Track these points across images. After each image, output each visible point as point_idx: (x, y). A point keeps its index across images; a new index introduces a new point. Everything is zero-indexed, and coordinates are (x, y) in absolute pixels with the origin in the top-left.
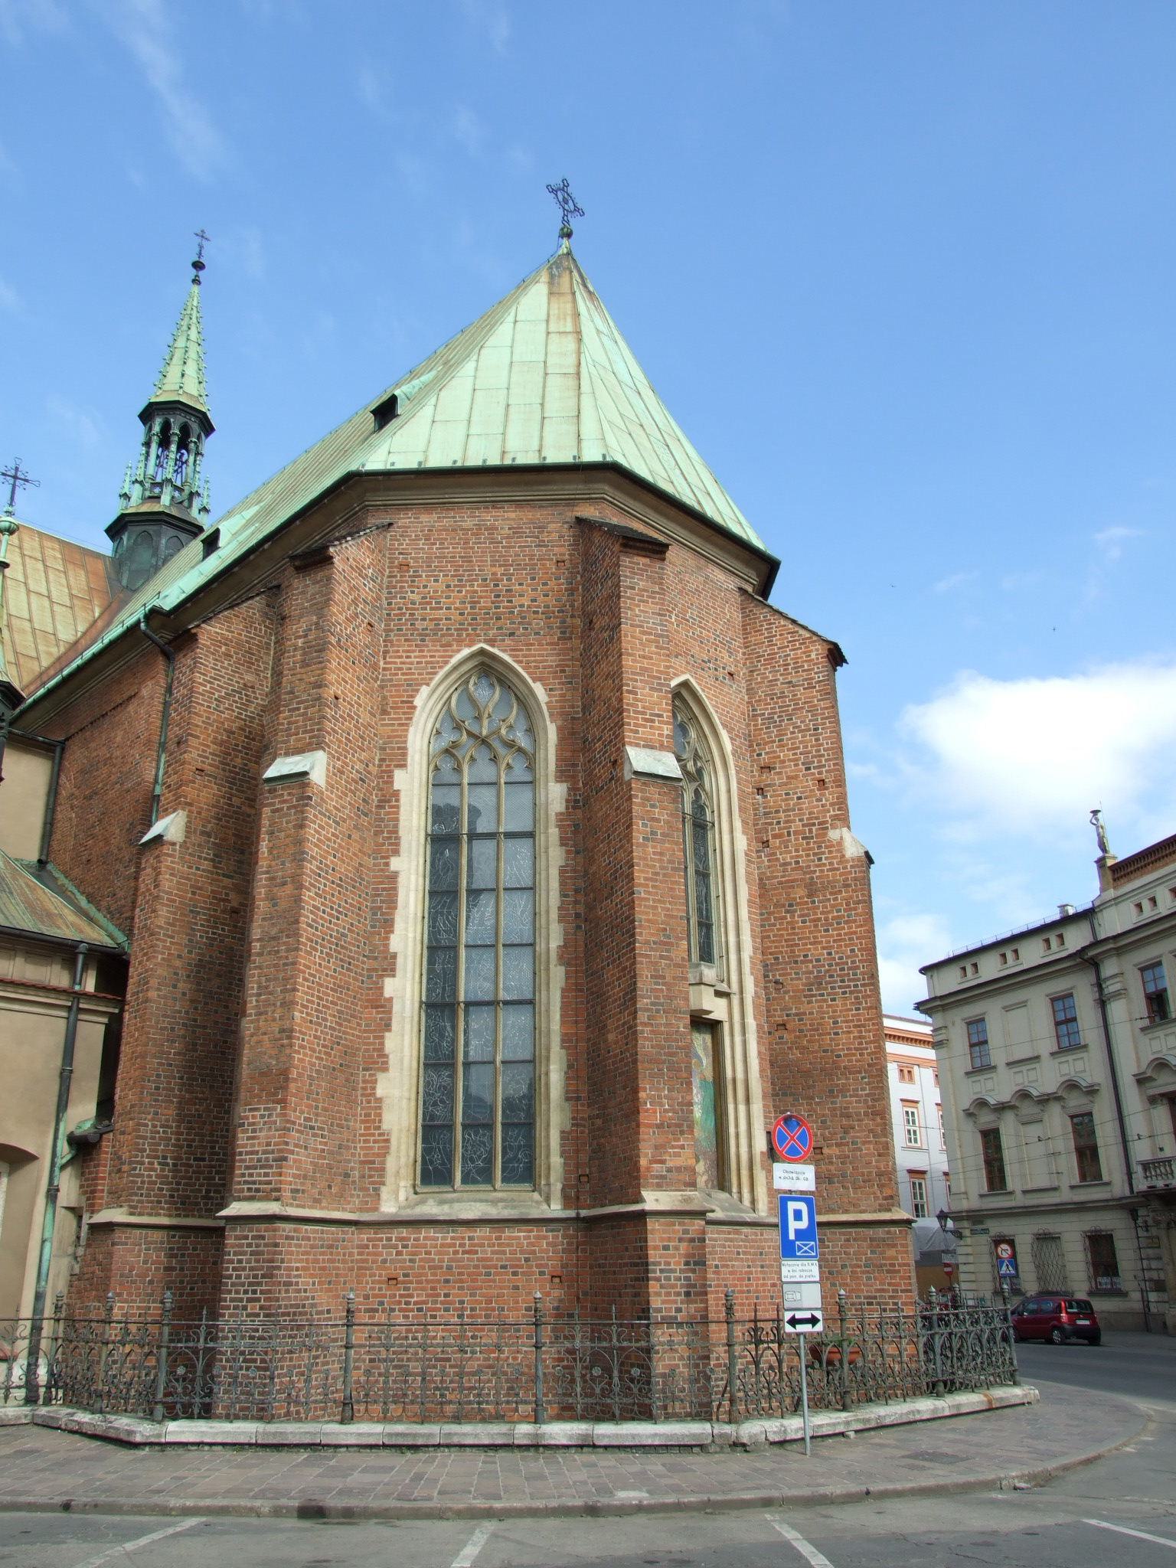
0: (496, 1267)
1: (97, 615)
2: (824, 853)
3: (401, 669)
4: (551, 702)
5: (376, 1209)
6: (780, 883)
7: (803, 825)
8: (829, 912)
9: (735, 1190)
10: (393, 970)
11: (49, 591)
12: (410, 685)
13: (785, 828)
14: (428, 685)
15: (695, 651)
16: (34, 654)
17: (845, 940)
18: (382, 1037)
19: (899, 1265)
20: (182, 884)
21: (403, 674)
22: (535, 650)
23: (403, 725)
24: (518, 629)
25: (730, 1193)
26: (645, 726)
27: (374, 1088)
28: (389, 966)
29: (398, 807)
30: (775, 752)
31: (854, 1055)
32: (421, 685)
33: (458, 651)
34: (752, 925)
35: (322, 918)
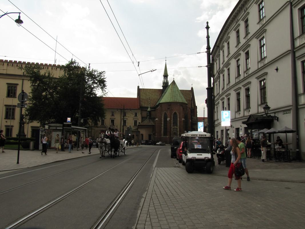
28: (162, 127)
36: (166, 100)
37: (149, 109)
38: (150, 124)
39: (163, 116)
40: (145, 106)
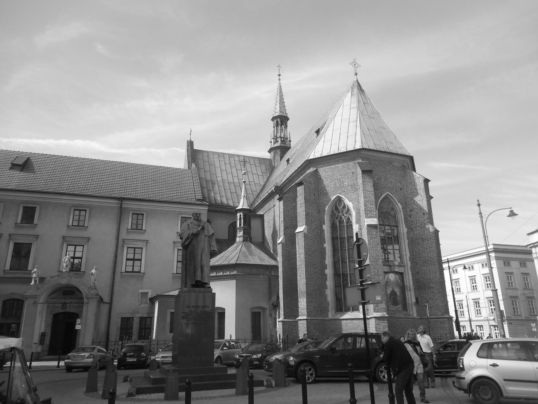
0: (352, 328)
2: (425, 231)
3: (322, 202)
4: (353, 206)
5: (328, 317)
6: (416, 239)
7: (420, 224)
8: (427, 245)
9: (408, 311)
10: (327, 268)
12: (324, 206)
13: (416, 225)
14: (328, 205)
15: (390, 185)
16: (255, 190)
17: (431, 252)
18: (326, 282)
19: (447, 328)
20: (286, 252)
21: (323, 203)
22: (349, 194)
23: (323, 215)
24: (345, 190)
25: (407, 311)
26: (369, 213)
27: (325, 293)
28: (325, 267)
29: (324, 233)
30: (413, 206)
31: (434, 279)
32: (326, 205)
33: (333, 197)
34: (409, 249)
35: (310, 260)
37: (242, 204)
39: (327, 218)
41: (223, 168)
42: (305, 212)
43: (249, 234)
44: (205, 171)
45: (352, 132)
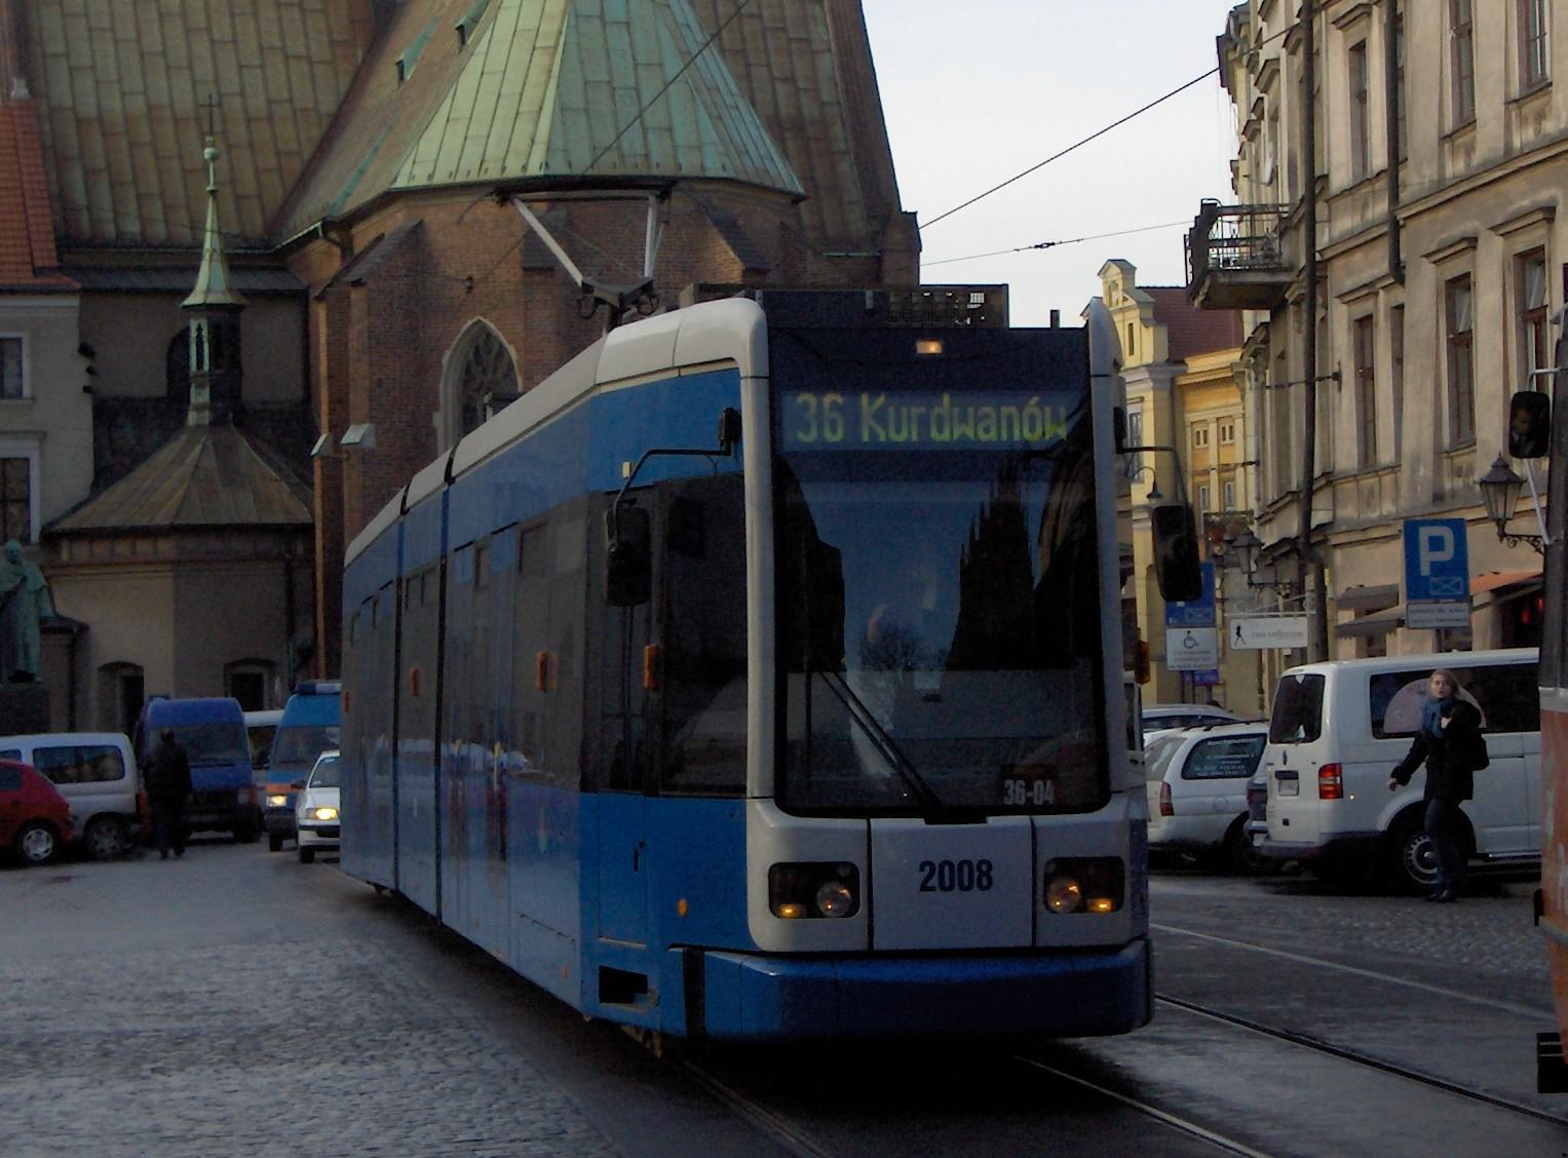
1: (360, 59)
11: (308, 48)
36: (495, 151)
38: (243, 509)
40: (133, 227)
41: (153, 42)
42: (367, 381)
43: (235, 393)
44: (70, 69)
45: (532, 95)
